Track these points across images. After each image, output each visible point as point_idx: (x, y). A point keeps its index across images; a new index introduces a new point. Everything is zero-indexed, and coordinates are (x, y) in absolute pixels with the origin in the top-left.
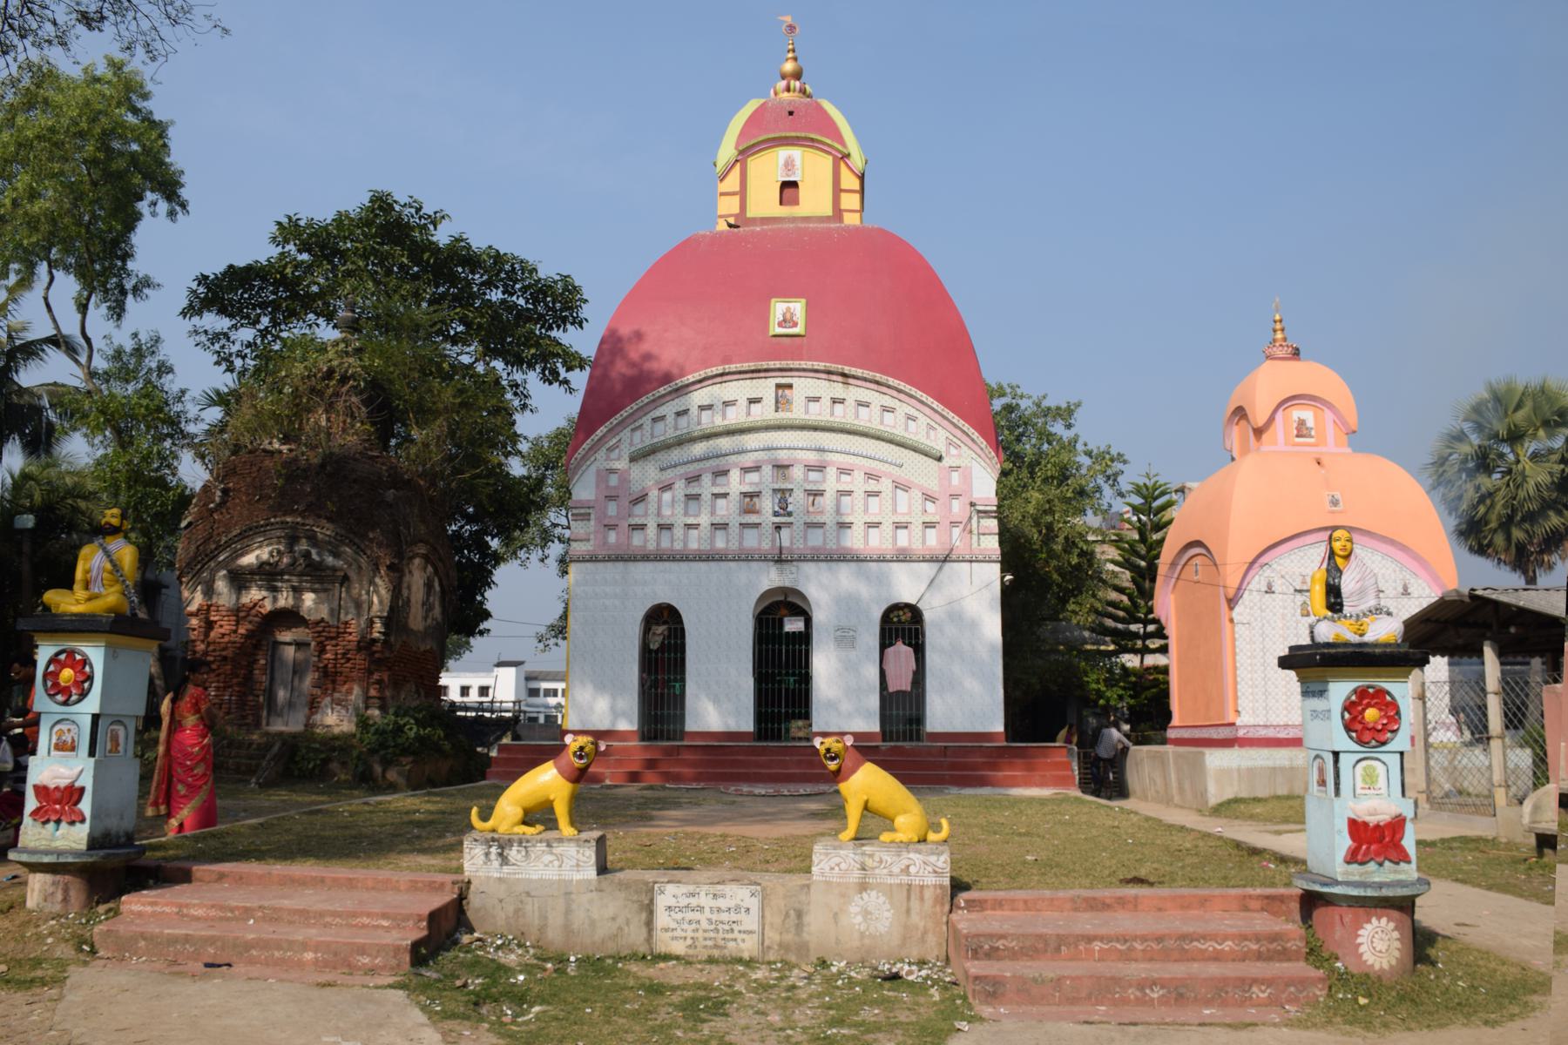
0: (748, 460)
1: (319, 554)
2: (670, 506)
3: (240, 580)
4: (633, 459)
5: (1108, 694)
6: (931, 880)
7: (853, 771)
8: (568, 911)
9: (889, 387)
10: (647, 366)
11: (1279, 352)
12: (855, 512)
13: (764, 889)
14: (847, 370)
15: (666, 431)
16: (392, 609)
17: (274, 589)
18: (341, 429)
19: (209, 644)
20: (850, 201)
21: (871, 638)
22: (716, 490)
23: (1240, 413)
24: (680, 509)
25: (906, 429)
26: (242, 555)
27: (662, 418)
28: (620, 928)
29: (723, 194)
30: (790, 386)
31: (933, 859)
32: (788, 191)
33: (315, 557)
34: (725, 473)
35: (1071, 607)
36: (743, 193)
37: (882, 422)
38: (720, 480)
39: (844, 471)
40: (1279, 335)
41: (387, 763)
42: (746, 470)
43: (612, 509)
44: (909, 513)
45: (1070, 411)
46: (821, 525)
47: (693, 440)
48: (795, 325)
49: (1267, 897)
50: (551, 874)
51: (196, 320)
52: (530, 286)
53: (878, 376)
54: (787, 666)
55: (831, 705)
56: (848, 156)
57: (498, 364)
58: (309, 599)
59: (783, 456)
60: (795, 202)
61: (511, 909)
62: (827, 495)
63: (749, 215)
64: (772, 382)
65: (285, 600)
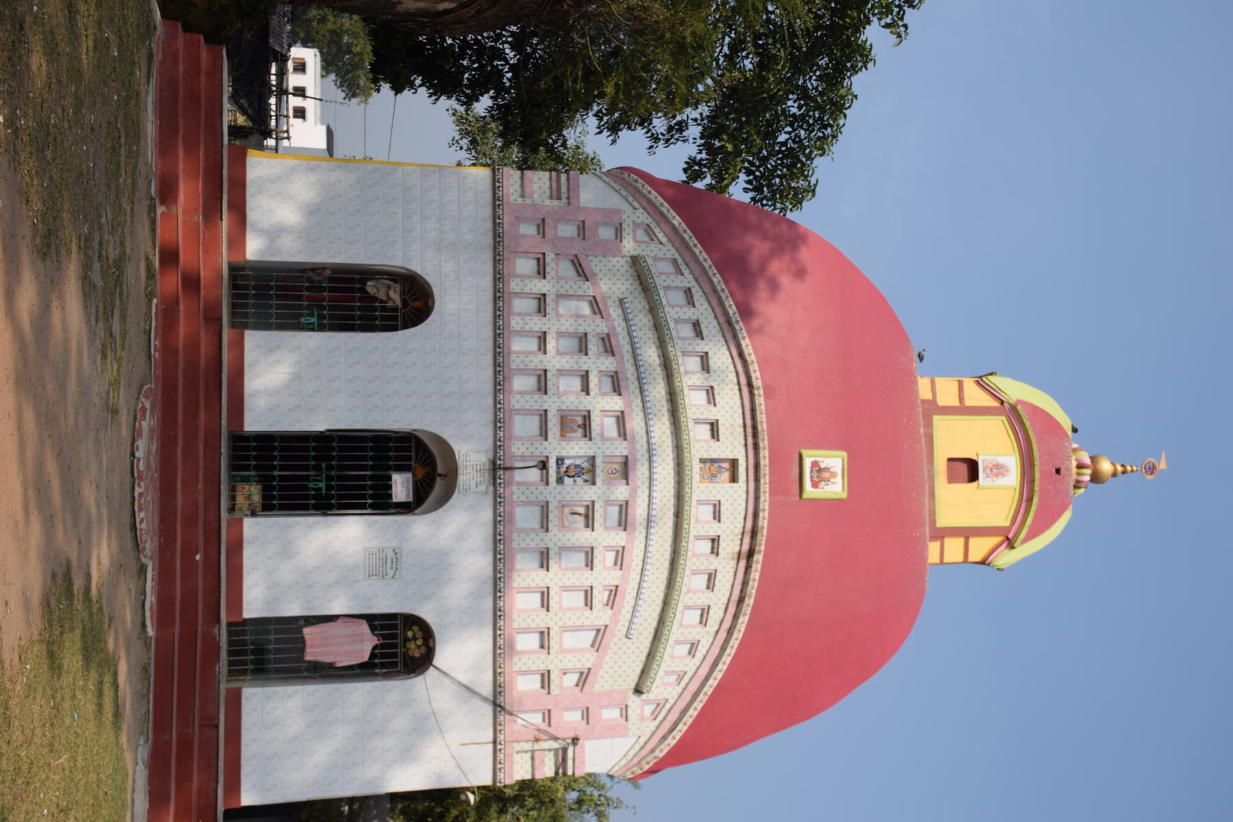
0: (635, 423)
2: (570, 314)
4: (635, 261)
9: (736, 617)
10: (762, 285)
12: (564, 576)
14: (758, 558)
15: (674, 309)
22: (594, 380)
24: (567, 325)
25: (678, 642)
27: (691, 302)
29: (960, 383)
30: (734, 479)
32: (963, 469)
34: (617, 389)
36: (962, 410)
37: (687, 607)
38: (607, 384)
39: (620, 557)
42: (621, 419)
43: (567, 230)
44: (562, 650)
46: (545, 527)
47: (662, 345)
48: (815, 485)
52: (803, 148)
53: (750, 601)
54: (340, 478)
56: (1011, 546)
57: (704, 109)
59: (641, 472)
60: (952, 479)
63: (936, 418)
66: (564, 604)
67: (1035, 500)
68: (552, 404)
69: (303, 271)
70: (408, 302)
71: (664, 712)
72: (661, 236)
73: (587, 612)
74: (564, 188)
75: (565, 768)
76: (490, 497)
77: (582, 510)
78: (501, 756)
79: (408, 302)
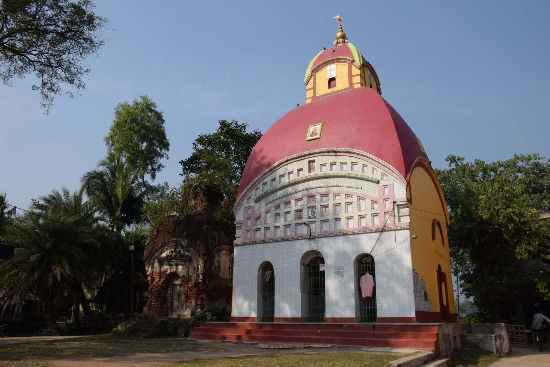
0: (299, 195)
1: (184, 251)
3: (161, 262)
9: (354, 153)
14: (335, 149)
15: (267, 188)
17: (170, 265)
21: (350, 271)
22: (286, 210)
26: (162, 253)
27: (266, 183)
30: (314, 161)
33: (182, 252)
36: (314, 88)
38: (288, 206)
39: (336, 195)
42: (298, 200)
43: (249, 223)
46: (327, 221)
48: (317, 134)
53: (349, 149)
55: (336, 303)
58: (180, 267)
59: (313, 191)
62: (330, 206)
65: (174, 269)
66: (364, 209)
71: (385, 172)
73: (353, 203)
75: (405, 204)
76: (319, 239)
78: (399, 228)
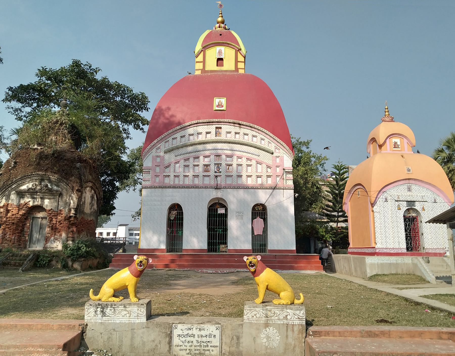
1: (51, 185)
3: (21, 194)
4: (165, 152)
5: (326, 236)
6: (297, 322)
7: (262, 272)
8: (132, 338)
9: (255, 128)
11: (387, 119)
13: (222, 326)
14: (240, 122)
15: (177, 143)
16: (78, 205)
17: (33, 198)
18: (61, 142)
19: (7, 218)
20: (241, 65)
22: (196, 164)
23: (374, 140)
24: (181, 170)
25: (261, 143)
26: (21, 186)
27: (176, 138)
28: (156, 346)
29: (197, 62)
30: (221, 128)
31: (298, 312)
33: (49, 186)
35: (314, 206)
36: (204, 62)
37: (252, 141)
38: (197, 160)
39: (239, 157)
40: (387, 113)
41: (73, 261)
43: (158, 169)
45: (308, 143)
46: (231, 176)
47: (187, 146)
48: (222, 106)
49: (451, 333)
50: (125, 320)
51: (8, 103)
52: (130, 96)
53: (251, 125)
54: (219, 226)
57: (119, 123)
58: (47, 202)
61: (106, 337)
64: (214, 127)
65: (38, 202)
67: (228, 42)
68: (201, 174)
69: (168, 235)
70: (176, 209)
72: (159, 146)
74: (147, 170)
77: (228, 167)
79: (176, 209)
